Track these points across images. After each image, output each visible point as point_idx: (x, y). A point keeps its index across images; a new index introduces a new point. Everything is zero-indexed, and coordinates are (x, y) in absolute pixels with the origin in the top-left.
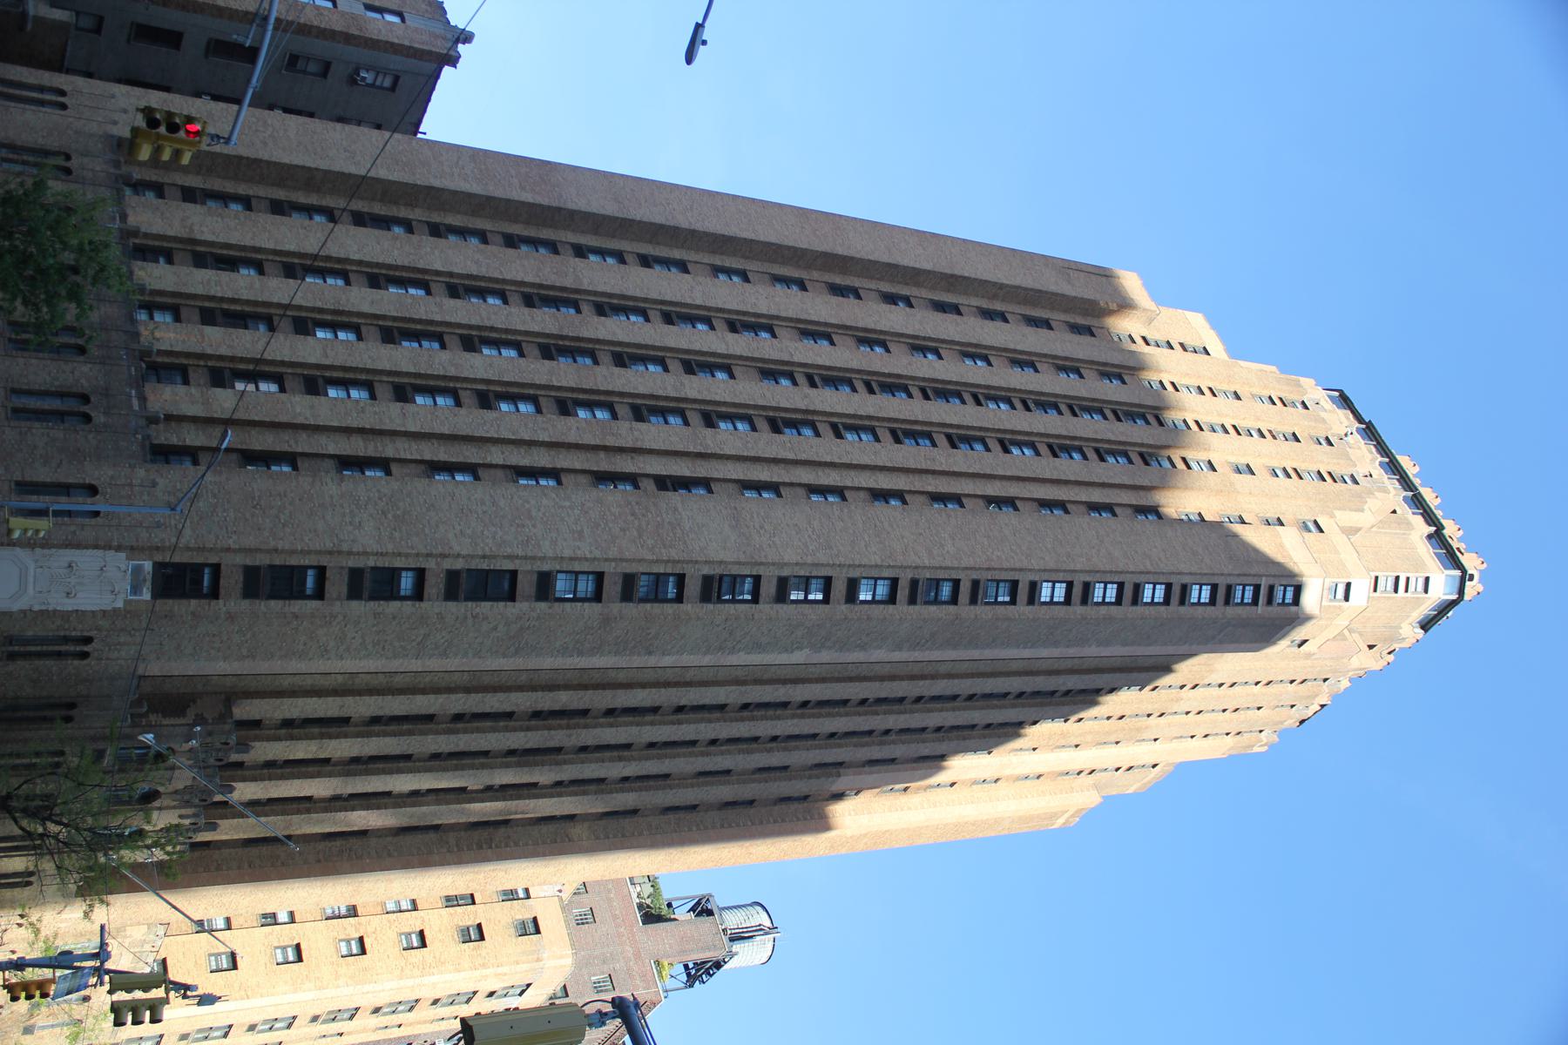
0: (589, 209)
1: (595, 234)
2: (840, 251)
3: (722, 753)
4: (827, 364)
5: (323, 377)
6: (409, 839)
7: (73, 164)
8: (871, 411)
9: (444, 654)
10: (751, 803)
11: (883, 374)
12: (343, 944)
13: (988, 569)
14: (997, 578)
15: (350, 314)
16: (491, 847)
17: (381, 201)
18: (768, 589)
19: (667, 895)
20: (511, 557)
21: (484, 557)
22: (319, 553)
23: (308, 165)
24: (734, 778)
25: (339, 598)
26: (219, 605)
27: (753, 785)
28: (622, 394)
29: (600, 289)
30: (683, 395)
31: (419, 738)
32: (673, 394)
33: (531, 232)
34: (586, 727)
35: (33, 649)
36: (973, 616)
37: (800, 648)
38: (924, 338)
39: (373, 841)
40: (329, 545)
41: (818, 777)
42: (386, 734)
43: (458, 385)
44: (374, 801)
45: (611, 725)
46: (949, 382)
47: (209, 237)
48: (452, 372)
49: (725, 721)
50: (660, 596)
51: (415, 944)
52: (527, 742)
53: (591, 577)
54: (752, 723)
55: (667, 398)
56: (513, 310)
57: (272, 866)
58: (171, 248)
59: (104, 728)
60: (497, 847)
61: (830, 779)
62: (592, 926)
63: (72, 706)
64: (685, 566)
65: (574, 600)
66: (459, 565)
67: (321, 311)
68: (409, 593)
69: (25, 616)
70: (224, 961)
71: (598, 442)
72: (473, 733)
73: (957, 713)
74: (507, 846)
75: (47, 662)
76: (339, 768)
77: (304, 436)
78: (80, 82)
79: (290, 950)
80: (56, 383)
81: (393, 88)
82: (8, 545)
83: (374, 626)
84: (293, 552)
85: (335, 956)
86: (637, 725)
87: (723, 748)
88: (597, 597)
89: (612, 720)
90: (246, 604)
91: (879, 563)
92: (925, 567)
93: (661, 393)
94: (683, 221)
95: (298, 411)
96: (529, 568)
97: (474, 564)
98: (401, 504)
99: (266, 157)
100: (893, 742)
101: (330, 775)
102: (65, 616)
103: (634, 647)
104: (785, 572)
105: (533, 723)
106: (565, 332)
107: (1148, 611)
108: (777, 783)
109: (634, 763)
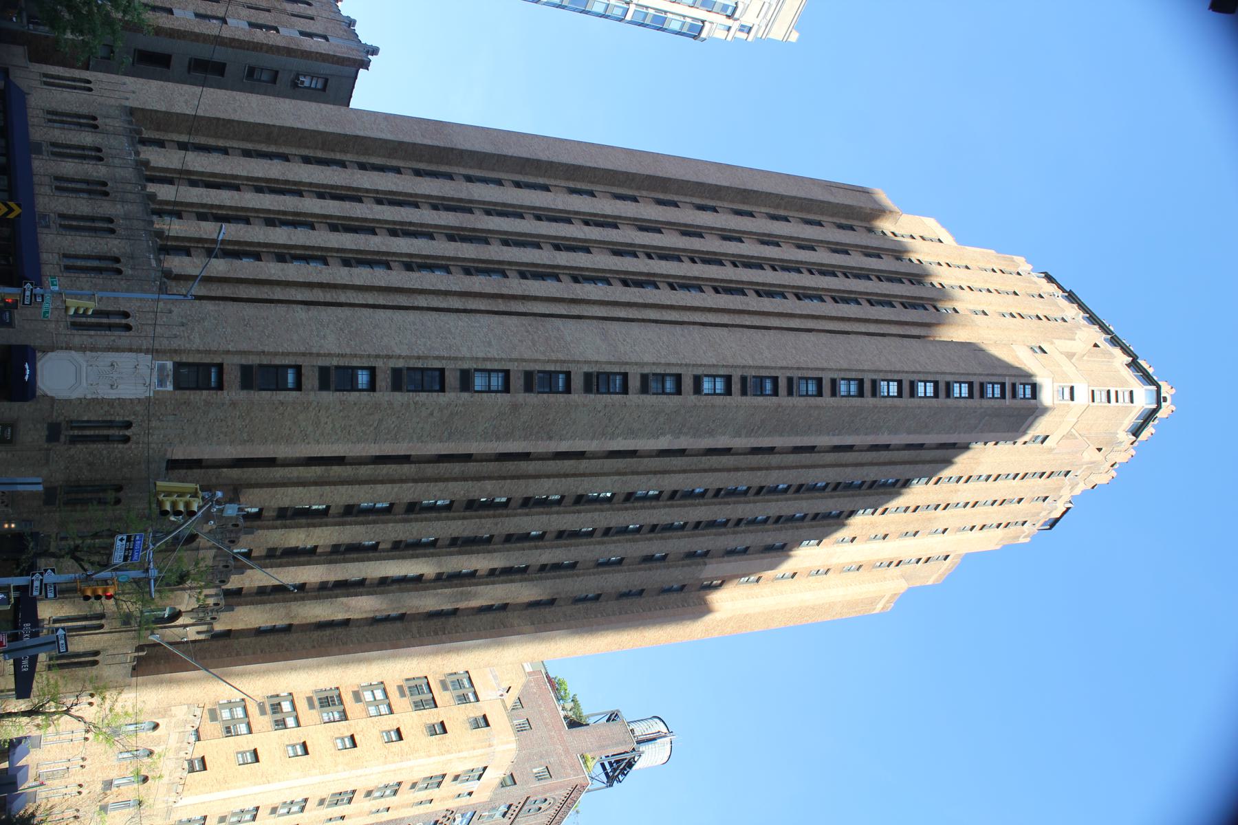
0: (473, 149)
1: (480, 169)
2: (660, 174)
3: (614, 542)
4: (660, 245)
5: (290, 254)
6: (381, 628)
7: (99, 122)
8: (697, 274)
9: (395, 439)
10: (641, 593)
11: (702, 252)
12: (339, 741)
13: (798, 369)
14: (806, 376)
15: (305, 214)
16: (444, 634)
17: (322, 149)
18: (634, 383)
19: (585, 711)
20: (437, 358)
21: (419, 358)
22: (295, 354)
23: (267, 123)
24: (625, 567)
25: (312, 389)
26: (225, 396)
27: (640, 573)
28: (510, 263)
29: (488, 199)
30: (555, 263)
31: (382, 526)
32: (548, 263)
33: (433, 168)
34: (507, 516)
35: (88, 433)
36: (791, 405)
37: (663, 434)
38: (730, 231)
39: (354, 630)
40: (302, 349)
41: (689, 565)
42: (356, 523)
43: (389, 259)
44: (352, 590)
45: (527, 515)
46: (752, 257)
47: (200, 169)
48: (384, 249)
49: (613, 510)
50: (553, 389)
51: (394, 739)
52: (464, 530)
53: (500, 375)
54: (634, 512)
55: (544, 266)
56: (425, 212)
57: (279, 651)
58: (173, 178)
59: (144, 509)
60: (449, 633)
61: (699, 568)
62: (530, 731)
63: (119, 488)
64: (570, 365)
65: (489, 391)
66: (400, 364)
67: (284, 213)
68: (365, 387)
69: (81, 403)
70: (249, 757)
71: (496, 291)
72: (422, 521)
73: (789, 502)
74: (456, 632)
75: (99, 446)
76: (323, 558)
77: (279, 289)
78: (101, 76)
79: (298, 747)
80: (96, 251)
81: (324, 89)
82: (66, 349)
83: (341, 411)
84: (276, 354)
85: (333, 751)
86: (547, 514)
87: (615, 538)
88: (506, 389)
89: (527, 510)
90: (243, 394)
91: (715, 363)
92: (750, 367)
93: (539, 262)
94: (543, 156)
95: (273, 272)
96: (453, 366)
97: (413, 364)
98: (354, 324)
99: (236, 119)
100: (743, 532)
101: (317, 563)
102: (111, 403)
103: (538, 432)
104: (646, 370)
105: (467, 513)
106: (464, 225)
107: (923, 402)
108: (659, 571)
109: (548, 551)
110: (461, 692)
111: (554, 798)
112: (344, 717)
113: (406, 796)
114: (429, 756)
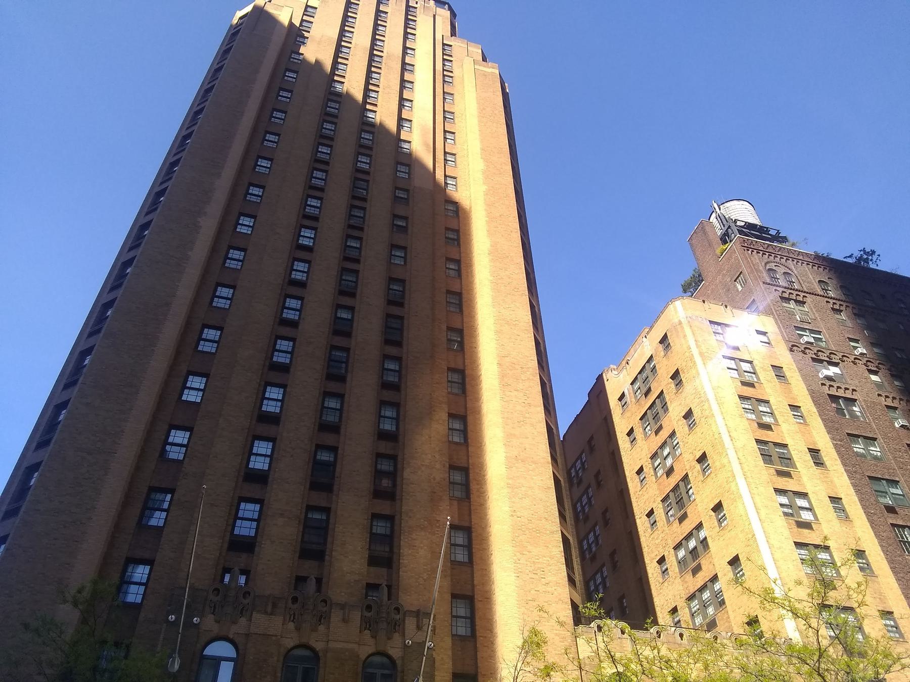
110: (650, 374)
111: (766, 264)
112: (685, 478)
113: (768, 390)
114: (699, 374)
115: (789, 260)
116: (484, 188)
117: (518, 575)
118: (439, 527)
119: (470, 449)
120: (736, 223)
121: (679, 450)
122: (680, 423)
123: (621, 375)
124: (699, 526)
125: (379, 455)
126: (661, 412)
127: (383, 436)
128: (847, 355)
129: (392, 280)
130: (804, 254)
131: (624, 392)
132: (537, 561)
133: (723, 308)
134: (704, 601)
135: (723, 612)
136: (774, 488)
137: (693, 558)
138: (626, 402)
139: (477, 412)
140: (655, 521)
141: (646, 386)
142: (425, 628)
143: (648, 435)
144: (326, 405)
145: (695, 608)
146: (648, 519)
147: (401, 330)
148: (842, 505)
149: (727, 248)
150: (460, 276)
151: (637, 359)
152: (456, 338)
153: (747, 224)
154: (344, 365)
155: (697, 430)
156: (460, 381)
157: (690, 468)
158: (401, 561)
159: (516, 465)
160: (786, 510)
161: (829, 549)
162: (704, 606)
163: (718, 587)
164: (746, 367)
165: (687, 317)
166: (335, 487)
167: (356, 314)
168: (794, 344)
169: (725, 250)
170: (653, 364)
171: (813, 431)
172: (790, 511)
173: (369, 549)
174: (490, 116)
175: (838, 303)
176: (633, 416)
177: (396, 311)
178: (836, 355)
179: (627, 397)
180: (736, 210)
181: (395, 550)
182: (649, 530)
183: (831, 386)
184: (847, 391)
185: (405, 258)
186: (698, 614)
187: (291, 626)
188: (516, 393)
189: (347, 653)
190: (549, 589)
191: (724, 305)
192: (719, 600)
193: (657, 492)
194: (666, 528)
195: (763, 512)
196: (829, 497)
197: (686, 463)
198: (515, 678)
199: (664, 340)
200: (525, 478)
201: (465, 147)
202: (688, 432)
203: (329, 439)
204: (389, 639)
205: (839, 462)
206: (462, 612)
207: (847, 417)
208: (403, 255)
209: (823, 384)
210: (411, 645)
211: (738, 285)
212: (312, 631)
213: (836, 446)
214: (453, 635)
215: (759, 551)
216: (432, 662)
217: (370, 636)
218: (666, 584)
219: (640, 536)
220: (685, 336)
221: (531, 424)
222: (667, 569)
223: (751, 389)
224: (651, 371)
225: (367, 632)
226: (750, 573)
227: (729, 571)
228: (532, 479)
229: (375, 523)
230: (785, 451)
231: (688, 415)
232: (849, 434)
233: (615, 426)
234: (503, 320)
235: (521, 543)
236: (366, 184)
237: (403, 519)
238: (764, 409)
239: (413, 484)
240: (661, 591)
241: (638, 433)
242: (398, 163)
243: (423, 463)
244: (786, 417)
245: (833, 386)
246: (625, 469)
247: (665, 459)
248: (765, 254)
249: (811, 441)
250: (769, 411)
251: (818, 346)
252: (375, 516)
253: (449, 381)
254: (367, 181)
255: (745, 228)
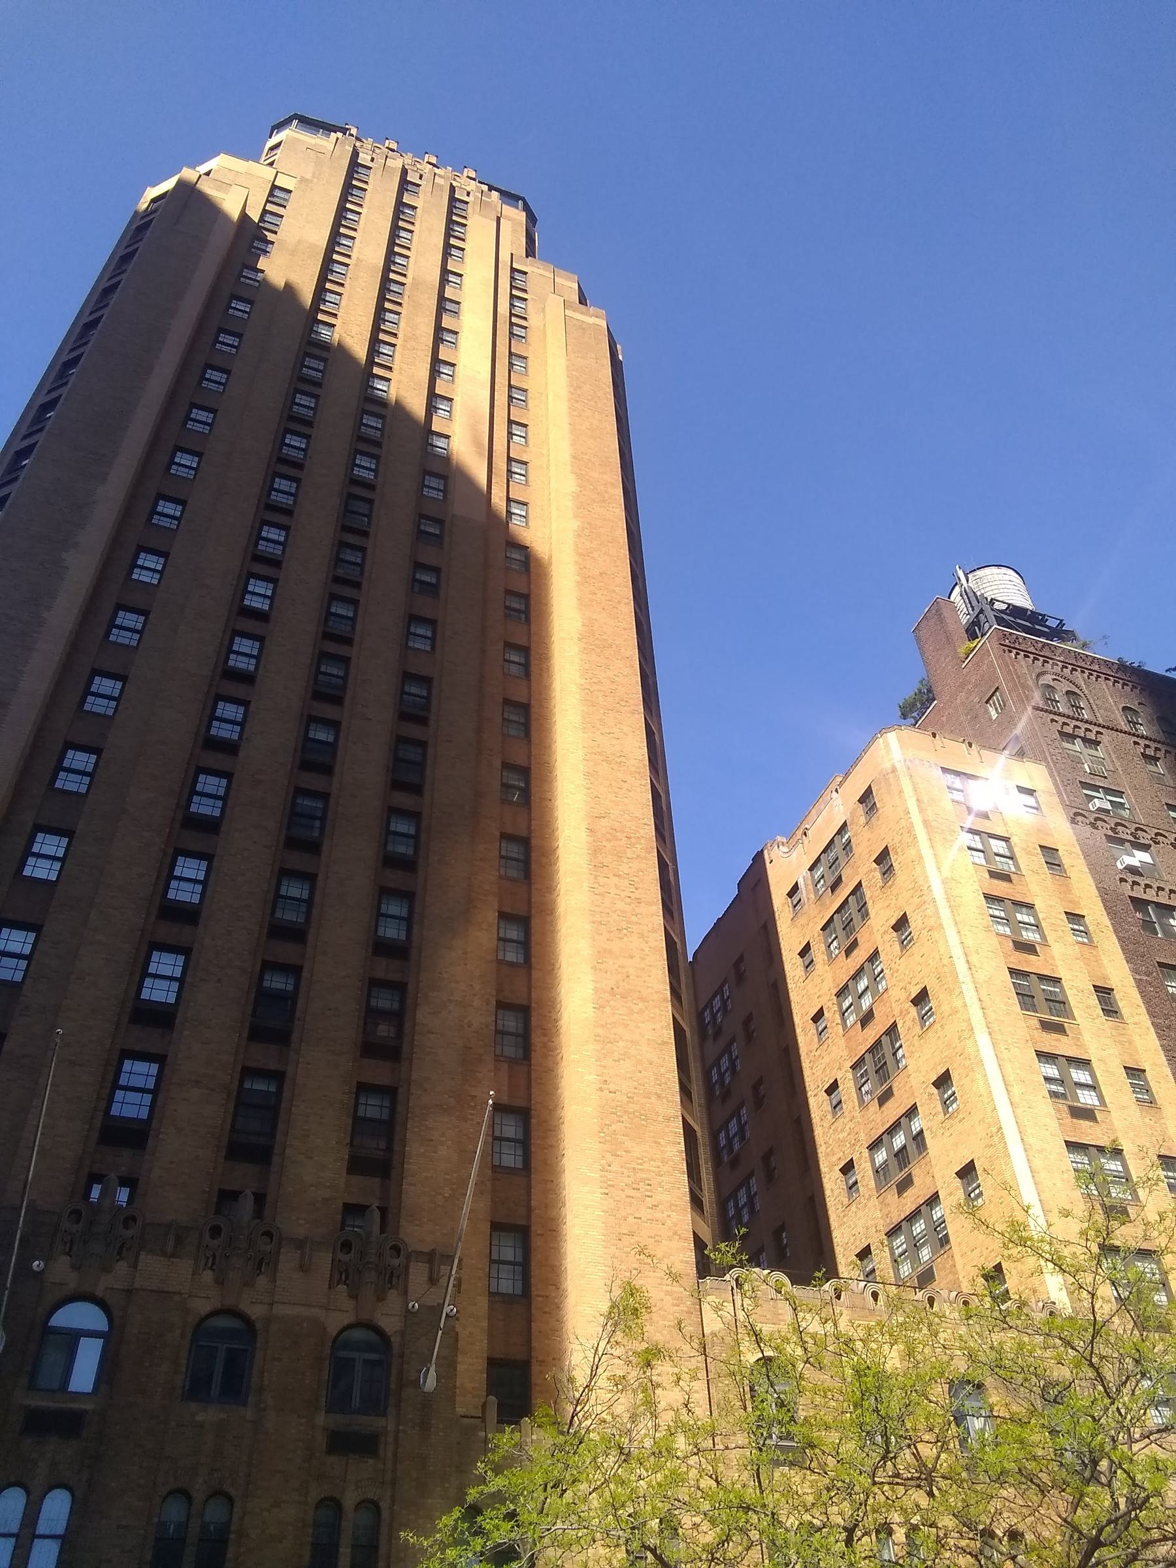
111: (1039, 676)
112: (892, 1031)
114: (921, 857)
115: (1076, 670)
116: (575, 524)
117: (607, 1191)
118: (474, 1108)
119: (534, 972)
120: (993, 605)
121: (884, 983)
122: (887, 937)
123: (794, 854)
124: (912, 1112)
125: (374, 983)
126: (857, 918)
127: (382, 948)
128: (1164, 833)
129: (408, 676)
130: (1103, 663)
131: (797, 882)
132: (640, 1167)
133: (964, 746)
134: (914, 1238)
135: (945, 1256)
136: (1036, 1051)
137: (900, 1164)
138: (800, 900)
139: (548, 910)
140: (840, 1102)
141: (833, 873)
142: (443, 1281)
143: (834, 956)
144: (283, 893)
145: (900, 1250)
146: (828, 1098)
147: (421, 766)
148: (1146, 1080)
149: (976, 646)
150: (528, 675)
151: (822, 828)
152: (517, 783)
153: (1011, 607)
154: (317, 823)
155: (915, 949)
156: (521, 857)
157: (901, 1013)
158: (405, 1166)
159: (612, 1003)
160: (1054, 1088)
161: (1121, 1154)
162: (915, 1245)
163: (939, 1215)
164: (998, 846)
165: (905, 761)
166: (295, 1037)
167: (341, 734)
168: (1078, 811)
169: (973, 650)
170: (847, 837)
171: (1103, 958)
172: (1061, 1089)
173: (351, 1144)
174: (589, 400)
175: (1153, 745)
176: (811, 925)
177: (413, 731)
178: (1146, 832)
179: (803, 892)
180: (994, 583)
181: (396, 1148)
182: (829, 1117)
183: (1135, 883)
184: (1160, 893)
185: (433, 639)
186: (905, 1259)
187: (208, 1276)
188: (616, 880)
189: (305, 1324)
190: (658, 1215)
191: (967, 742)
192: (940, 1236)
193: (845, 1053)
194: (857, 1114)
195: (1016, 1091)
196: (1125, 1067)
197: (893, 1005)
198: (595, 1367)
199: (866, 797)
200: (626, 1026)
201: (544, 452)
202: (899, 953)
203: (286, 951)
204: (381, 1298)
205: (1143, 1010)
206: (508, 1254)
207: (1159, 935)
208: (429, 634)
209: (1122, 880)
210: (414, 1313)
211: (990, 708)
212: (244, 1285)
213: (1139, 983)
214: (491, 1294)
215: (1008, 1156)
216: (453, 1338)
217: (346, 1294)
218: (853, 1208)
219: (815, 1126)
220: (901, 792)
221: (639, 933)
222: (856, 1183)
223: (1004, 884)
224: (844, 849)
225: (342, 1288)
226: (991, 1192)
227: (957, 1188)
228: (637, 1027)
229: (362, 1100)
230: (1056, 990)
231: (901, 924)
232: (1161, 965)
233: (781, 939)
234: (599, 753)
235: (613, 1136)
236: (367, 506)
237: (413, 1094)
238: (1026, 919)
239: (433, 1033)
240: (845, 1219)
241: (818, 952)
242: (427, 473)
243: (451, 998)
244: (1060, 933)
245: (1139, 884)
246: (794, 1012)
247: (859, 998)
248: (1038, 660)
249: (1100, 974)
250: (1033, 921)
251: (1117, 815)
252: (363, 1088)
253: (502, 857)
254: (370, 502)
255: (1006, 614)
